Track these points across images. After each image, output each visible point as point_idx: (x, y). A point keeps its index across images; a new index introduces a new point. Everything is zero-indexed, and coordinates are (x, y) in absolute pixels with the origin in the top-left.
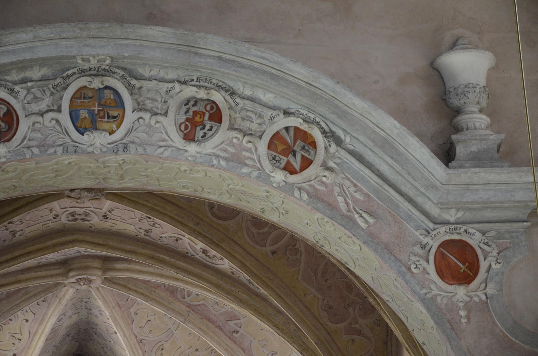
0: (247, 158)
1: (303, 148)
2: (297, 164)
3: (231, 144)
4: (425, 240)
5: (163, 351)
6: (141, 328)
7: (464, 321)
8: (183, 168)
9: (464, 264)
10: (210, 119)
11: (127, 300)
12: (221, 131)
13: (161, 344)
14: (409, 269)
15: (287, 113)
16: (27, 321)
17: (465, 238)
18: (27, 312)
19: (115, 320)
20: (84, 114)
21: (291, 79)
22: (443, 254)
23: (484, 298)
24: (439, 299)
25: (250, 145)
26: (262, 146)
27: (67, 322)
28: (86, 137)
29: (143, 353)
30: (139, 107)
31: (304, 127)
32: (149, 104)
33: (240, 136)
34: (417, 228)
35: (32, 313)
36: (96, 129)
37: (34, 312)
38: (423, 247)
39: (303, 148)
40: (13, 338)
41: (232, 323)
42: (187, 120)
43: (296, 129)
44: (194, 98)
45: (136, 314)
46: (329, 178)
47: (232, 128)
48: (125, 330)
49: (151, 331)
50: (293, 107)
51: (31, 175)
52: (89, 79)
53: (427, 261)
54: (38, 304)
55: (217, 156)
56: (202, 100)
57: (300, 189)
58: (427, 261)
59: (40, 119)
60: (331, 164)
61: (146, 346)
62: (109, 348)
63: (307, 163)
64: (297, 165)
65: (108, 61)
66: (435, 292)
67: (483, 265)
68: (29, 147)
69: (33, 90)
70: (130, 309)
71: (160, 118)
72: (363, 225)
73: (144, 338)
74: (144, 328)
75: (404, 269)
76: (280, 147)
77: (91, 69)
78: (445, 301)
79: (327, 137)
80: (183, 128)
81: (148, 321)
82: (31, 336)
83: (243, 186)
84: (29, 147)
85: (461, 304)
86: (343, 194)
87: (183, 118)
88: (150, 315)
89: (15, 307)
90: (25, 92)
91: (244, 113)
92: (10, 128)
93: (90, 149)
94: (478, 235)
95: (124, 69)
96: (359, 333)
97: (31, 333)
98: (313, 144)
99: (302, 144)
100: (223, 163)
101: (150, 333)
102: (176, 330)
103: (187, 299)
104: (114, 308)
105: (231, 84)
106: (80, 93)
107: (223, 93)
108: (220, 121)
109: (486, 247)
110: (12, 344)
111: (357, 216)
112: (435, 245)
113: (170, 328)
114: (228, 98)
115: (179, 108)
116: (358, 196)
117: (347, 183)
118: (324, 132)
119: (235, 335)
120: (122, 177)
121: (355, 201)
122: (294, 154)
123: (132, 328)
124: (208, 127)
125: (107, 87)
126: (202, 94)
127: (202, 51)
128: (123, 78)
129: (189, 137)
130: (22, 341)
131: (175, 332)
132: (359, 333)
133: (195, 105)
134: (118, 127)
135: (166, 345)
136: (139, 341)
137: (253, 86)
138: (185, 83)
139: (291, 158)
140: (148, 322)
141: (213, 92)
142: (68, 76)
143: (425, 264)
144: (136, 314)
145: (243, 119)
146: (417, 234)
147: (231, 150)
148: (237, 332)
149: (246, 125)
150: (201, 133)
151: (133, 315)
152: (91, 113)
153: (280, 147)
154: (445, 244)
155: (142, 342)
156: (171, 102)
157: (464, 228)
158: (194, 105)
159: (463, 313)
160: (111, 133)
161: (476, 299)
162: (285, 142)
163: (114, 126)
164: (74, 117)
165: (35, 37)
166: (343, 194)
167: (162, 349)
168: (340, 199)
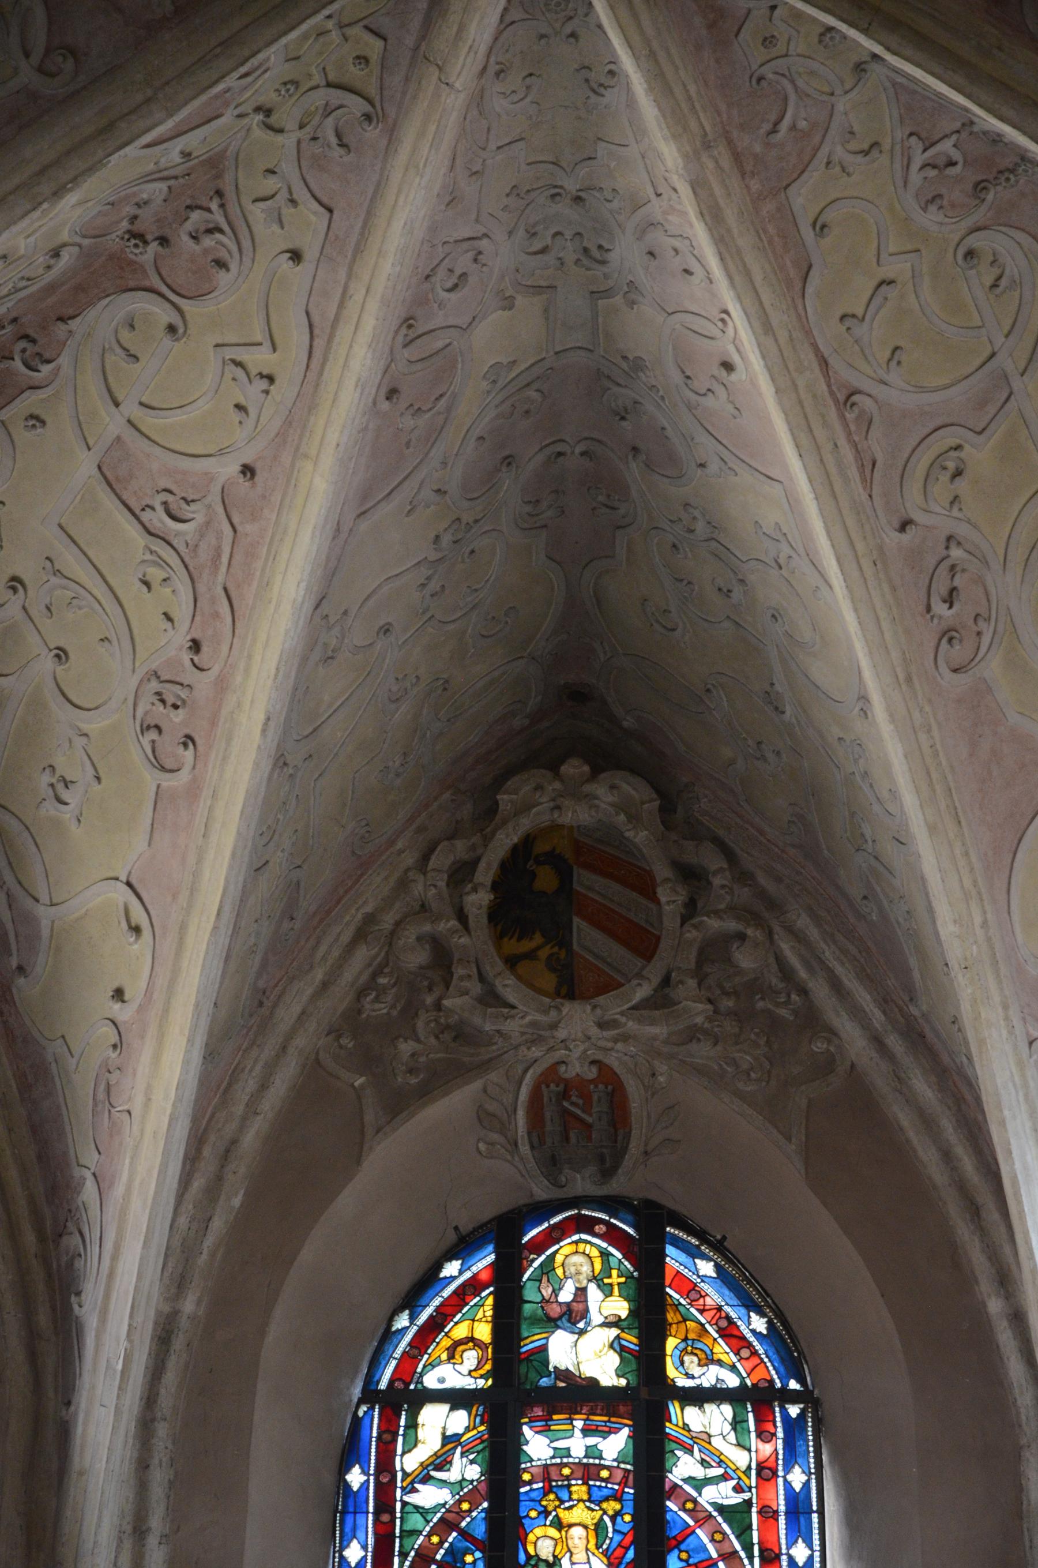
5: (962, 486)
6: (849, 322)
11: (774, 131)
13: (953, 442)
16: (296, 256)
18: (293, 202)
19: (712, 216)
29: (862, 468)
35: (315, 205)
37: (325, 200)
40: (240, 373)
45: (821, 228)
48: (766, 297)
49: (896, 348)
54: (342, 145)
61: (876, 432)
62: (700, 526)
70: (792, 190)
73: (865, 385)
74: (865, 325)
81: (882, 283)
82: (319, 343)
88: (892, 249)
89: (218, 50)
97: (316, 331)
101: (894, 363)
102: (1022, 375)
104: (707, 146)
110: (232, 408)
113: (993, 355)
123: (800, 307)
130: (277, 382)
131: (1017, 383)
136: (841, 397)
140: (884, 288)
144: (821, 228)
151: (808, 234)
155: (853, 404)
167: (958, 473)
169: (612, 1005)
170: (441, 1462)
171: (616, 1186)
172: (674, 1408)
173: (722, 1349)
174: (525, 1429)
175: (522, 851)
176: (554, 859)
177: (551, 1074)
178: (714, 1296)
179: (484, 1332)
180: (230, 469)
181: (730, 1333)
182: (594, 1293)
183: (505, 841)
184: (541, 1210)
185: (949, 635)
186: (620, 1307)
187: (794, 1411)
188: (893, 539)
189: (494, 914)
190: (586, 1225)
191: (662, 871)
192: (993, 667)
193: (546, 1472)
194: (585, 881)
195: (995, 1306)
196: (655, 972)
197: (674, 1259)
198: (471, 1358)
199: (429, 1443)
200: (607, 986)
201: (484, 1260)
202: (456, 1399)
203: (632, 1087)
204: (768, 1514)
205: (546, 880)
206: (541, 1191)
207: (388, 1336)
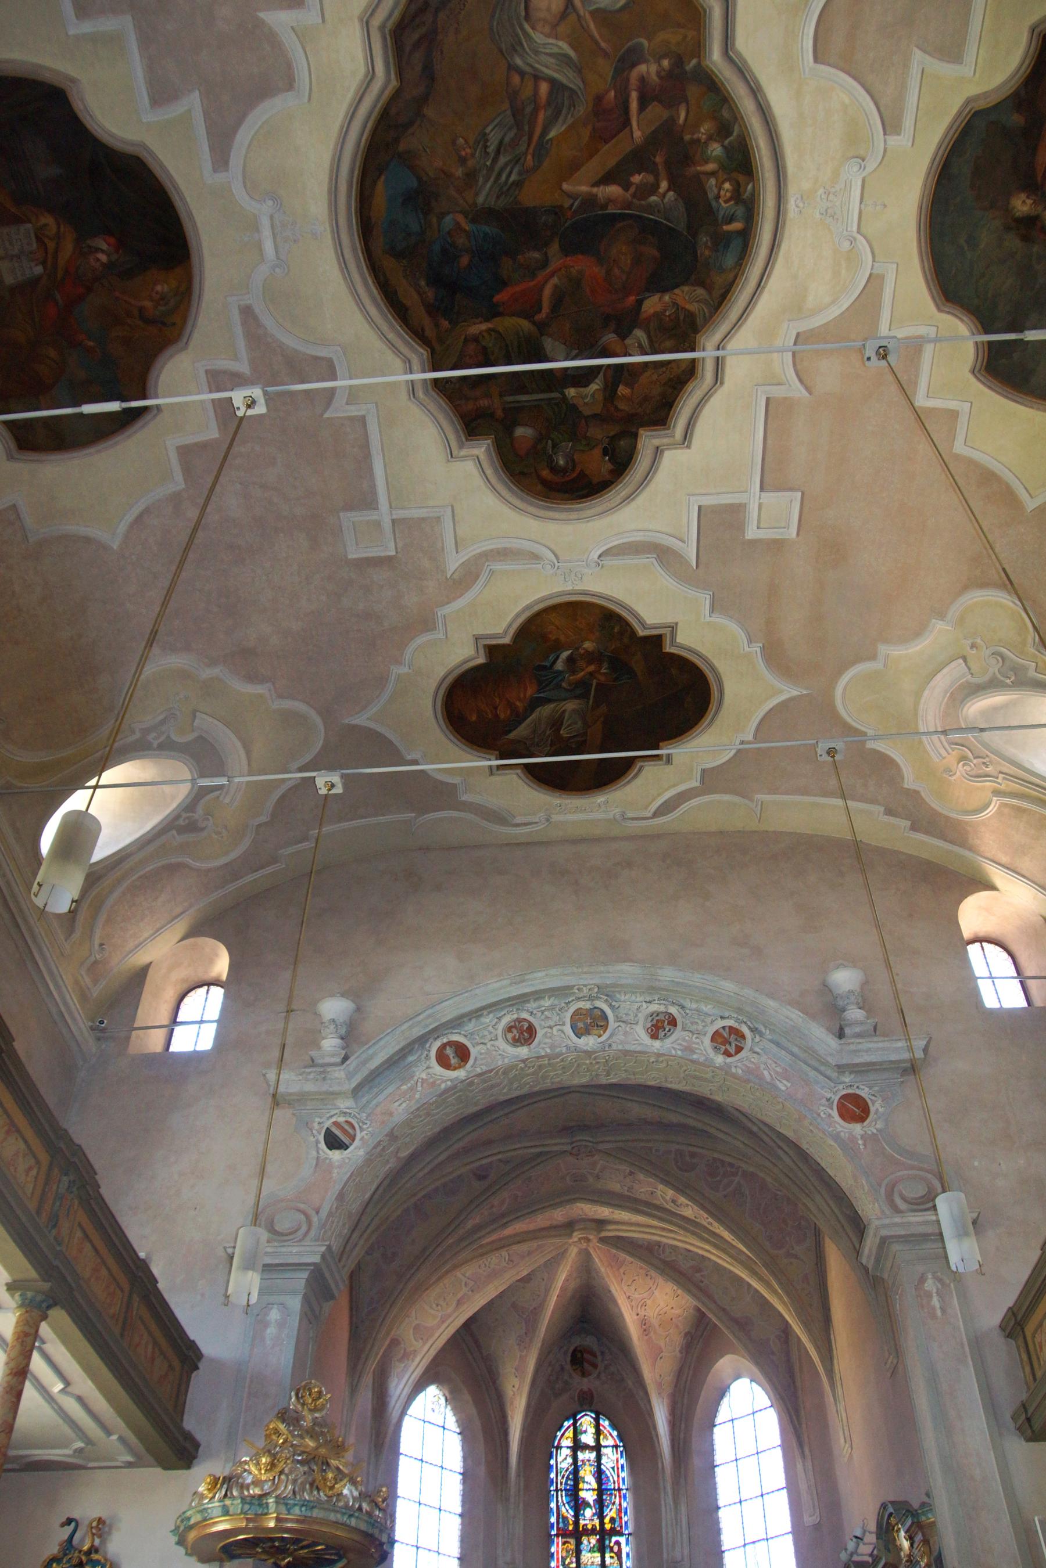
0: (696, 1049)
1: (736, 1039)
2: (732, 1050)
3: (684, 1040)
4: (829, 1096)
7: (861, 1147)
8: (651, 1060)
9: (858, 1109)
10: (669, 1024)
12: (676, 1032)
14: (819, 1115)
15: (722, 1018)
17: (858, 1092)
20: (580, 1025)
21: (723, 992)
22: (844, 1105)
23: (875, 1131)
24: (842, 1134)
25: (698, 1040)
26: (707, 1041)
27: (573, 1285)
28: (582, 1039)
30: (618, 1019)
31: (736, 1025)
32: (625, 1018)
33: (690, 1035)
34: (823, 1088)
36: (589, 1034)
38: (828, 1100)
39: (736, 1039)
41: (698, 1275)
42: (652, 1025)
43: (730, 1028)
44: (655, 1012)
45: (624, 1274)
46: (755, 1058)
47: (684, 1029)
50: (726, 1014)
51: (546, 1072)
52: (584, 1003)
53: (832, 1109)
55: (674, 1049)
56: (662, 1013)
57: (736, 1067)
58: (832, 1109)
59: (549, 1030)
60: (758, 1050)
63: (739, 1049)
64: (732, 1050)
65: (596, 990)
66: (839, 1129)
67: (872, 1109)
68: (543, 1048)
69: (546, 1013)
71: (634, 1026)
72: (783, 1088)
75: (815, 1115)
76: (720, 1040)
77: (584, 997)
78: (847, 1135)
79: (752, 1031)
80: (650, 1031)
83: (695, 1071)
84: (543, 1048)
85: (859, 1137)
86: (767, 1068)
87: (649, 1025)
90: (540, 1014)
91: (691, 1020)
92: (531, 1036)
93: (585, 1048)
94: (867, 1089)
95: (607, 995)
96: (796, 1257)
98: (743, 1037)
99: (735, 1037)
100: (679, 1053)
103: (662, 1256)
105: (682, 1001)
106: (577, 1013)
107: (677, 1007)
108: (675, 1025)
109: (873, 1098)
111: (778, 1082)
112: (836, 1099)
114: (680, 1010)
115: (646, 1018)
116: (778, 1069)
117: (770, 1061)
118: (750, 1028)
119: (701, 1284)
120: (608, 1075)
121: (777, 1073)
122: (730, 1044)
124: (667, 1029)
125: (595, 1008)
126: (662, 1009)
127: (660, 978)
128: (606, 1001)
129: (654, 1036)
132: (796, 1257)
133: (657, 1015)
134: (604, 1033)
135: (649, 1302)
137: (697, 1001)
138: (650, 1002)
139: (728, 1046)
141: (670, 1007)
142: (569, 1002)
143: (830, 1111)
145: (692, 1023)
146: (823, 1092)
147: (685, 1044)
148: (702, 1282)
149: (694, 1028)
150: (663, 1033)
152: (586, 1024)
153: (720, 1040)
154: (845, 1097)
156: (640, 1015)
157: (856, 1085)
158: (657, 1015)
159: (860, 1142)
160: (600, 1036)
161: (870, 1133)
162: (724, 1037)
163: (602, 1032)
164: (573, 1027)
165: (547, 975)
166: (767, 1068)
168: (766, 1073)
169: (591, 1377)
170: (566, 1459)
171: (592, 1408)
172: (602, 1449)
173: (610, 1437)
174: (579, 1453)
175: (575, 1351)
176: (581, 1351)
177: (581, 1390)
178: (608, 1428)
179: (571, 1435)
180: (532, 1308)
181: (611, 1434)
182: (589, 1427)
183: (572, 1349)
184: (580, 1412)
185: (645, 1330)
186: (593, 1430)
187: (622, 1449)
188: (636, 1317)
189: (572, 1361)
190: (586, 1415)
191: (598, 1354)
192: (652, 1334)
193: (583, 1461)
194: (585, 1355)
195: (653, 1433)
196: (598, 1371)
197: (601, 1422)
198: (570, 1440)
199: (563, 1457)
200: (590, 1375)
201: (571, 1421)
202: (568, 1447)
203: (595, 1396)
204: (618, 1469)
205: (579, 1355)
206: (579, 1409)
207: (556, 1436)
